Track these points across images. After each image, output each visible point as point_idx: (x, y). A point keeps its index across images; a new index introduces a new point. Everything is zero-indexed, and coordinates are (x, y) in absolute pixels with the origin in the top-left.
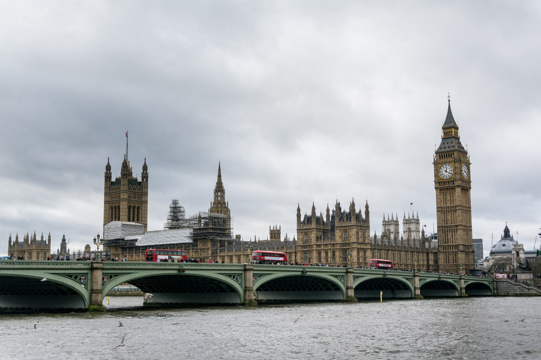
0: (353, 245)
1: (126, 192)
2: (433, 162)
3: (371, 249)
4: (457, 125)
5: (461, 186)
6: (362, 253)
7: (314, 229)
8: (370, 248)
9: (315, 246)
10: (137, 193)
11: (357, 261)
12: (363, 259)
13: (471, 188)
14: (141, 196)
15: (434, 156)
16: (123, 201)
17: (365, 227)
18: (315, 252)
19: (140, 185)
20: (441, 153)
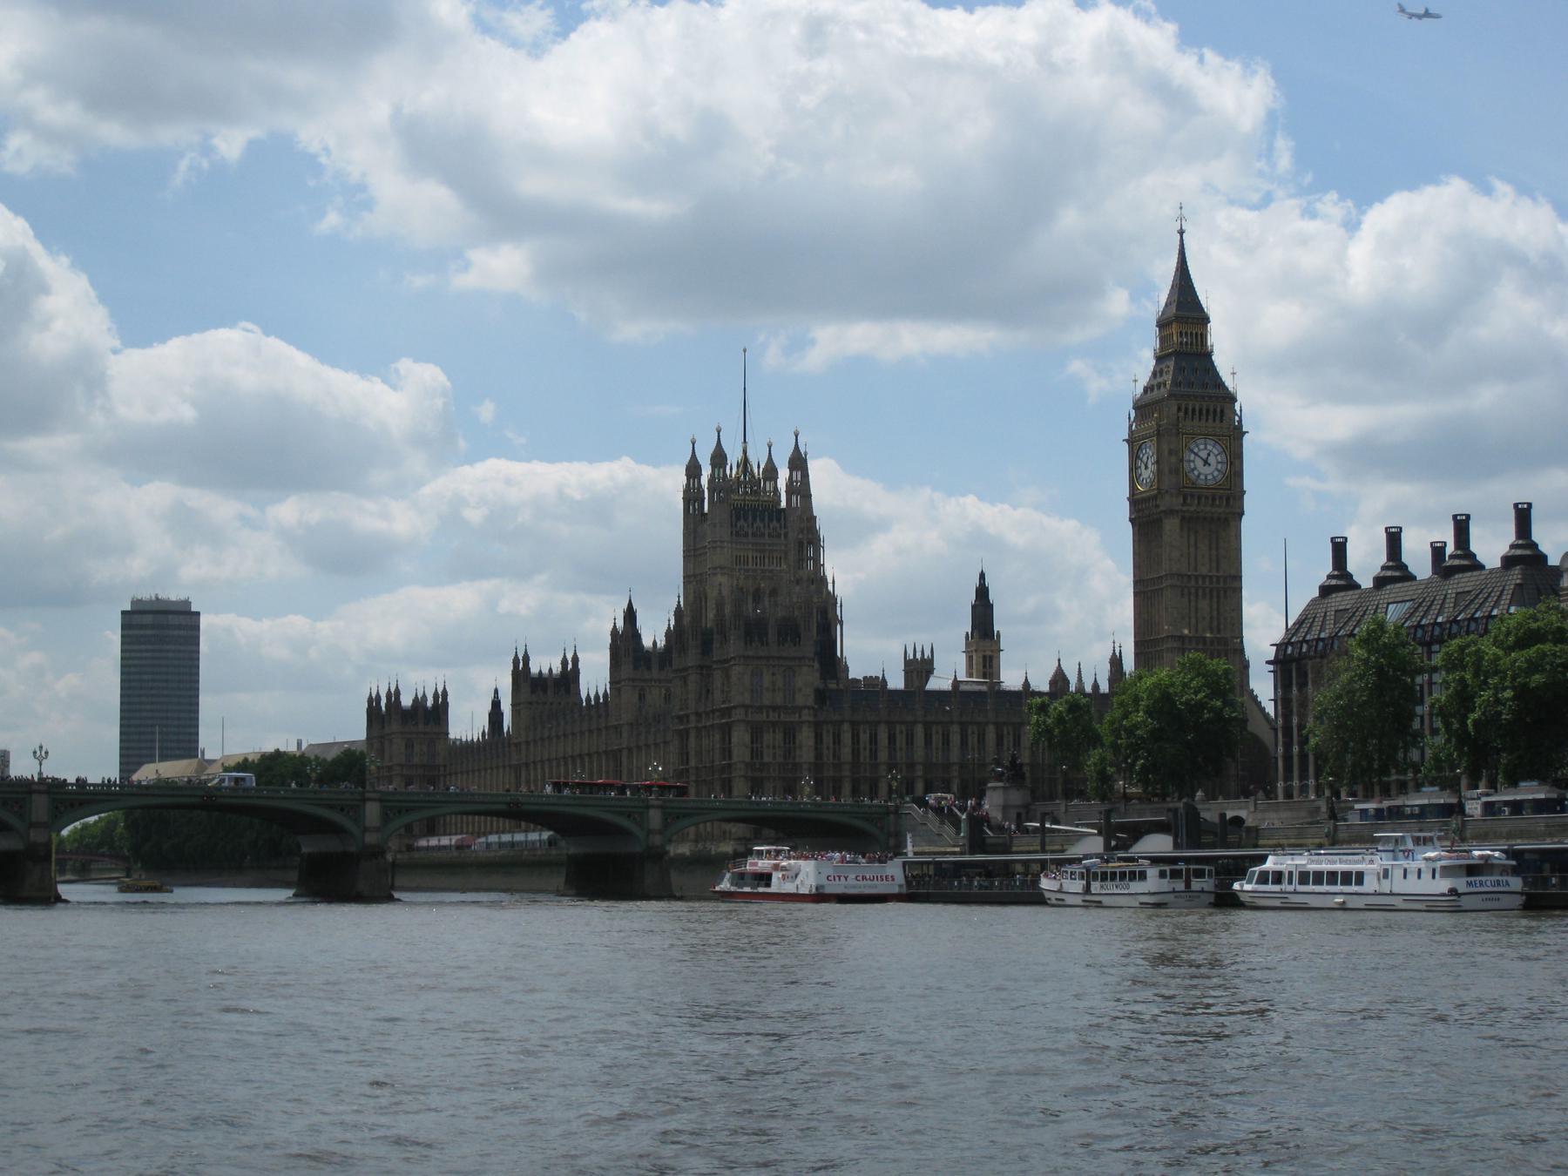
0: (736, 714)
1: (721, 547)
2: (1127, 437)
3: (817, 726)
4: (1203, 309)
5: (1177, 511)
6: (771, 734)
7: (692, 667)
8: (809, 722)
9: (693, 718)
10: (767, 547)
11: (748, 759)
12: (775, 754)
13: (1242, 514)
14: (783, 556)
15: (1129, 418)
16: (715, 574)
17: (794, 659)
18: (693, 734)
19: (779, 520)
20: (1146, 405)
